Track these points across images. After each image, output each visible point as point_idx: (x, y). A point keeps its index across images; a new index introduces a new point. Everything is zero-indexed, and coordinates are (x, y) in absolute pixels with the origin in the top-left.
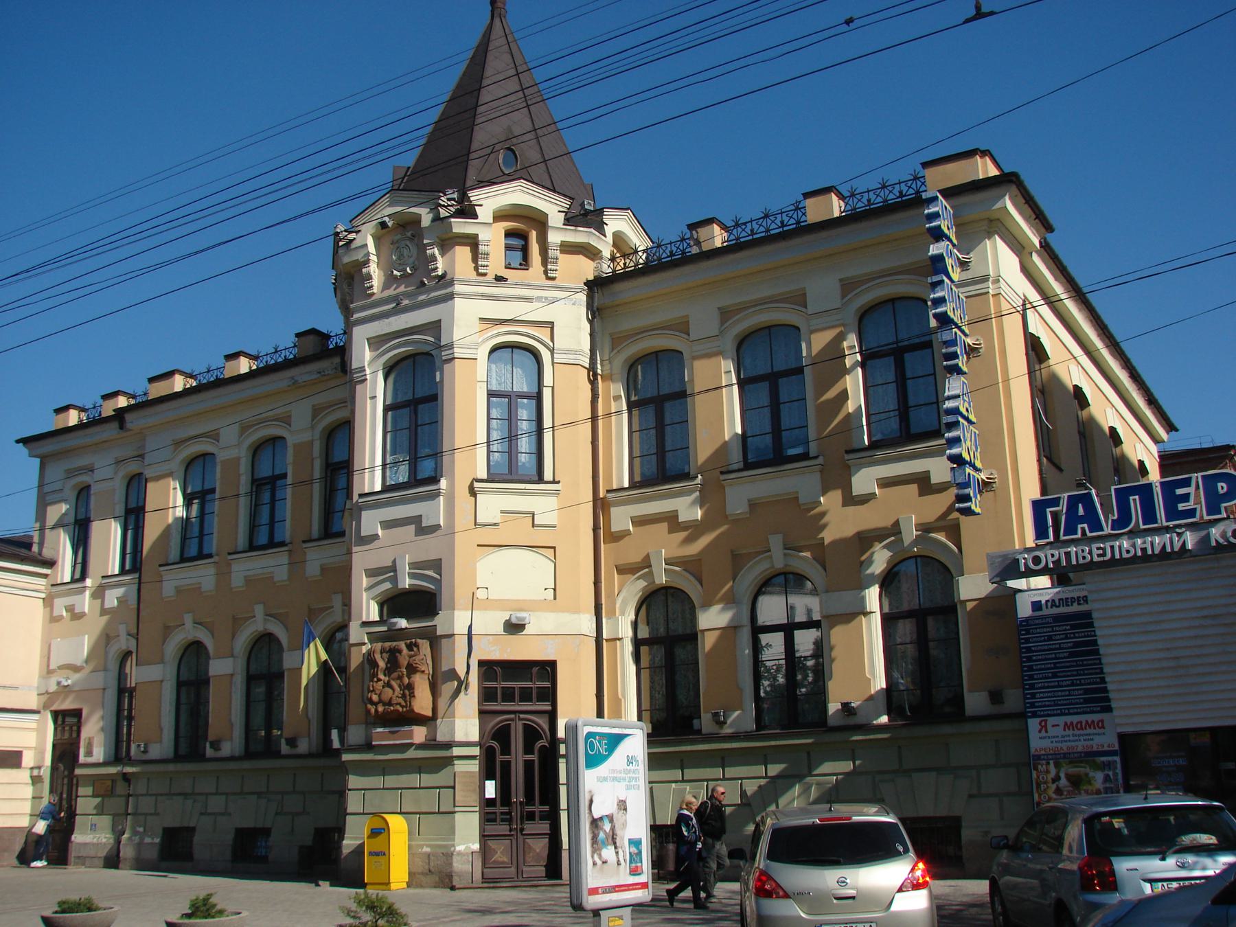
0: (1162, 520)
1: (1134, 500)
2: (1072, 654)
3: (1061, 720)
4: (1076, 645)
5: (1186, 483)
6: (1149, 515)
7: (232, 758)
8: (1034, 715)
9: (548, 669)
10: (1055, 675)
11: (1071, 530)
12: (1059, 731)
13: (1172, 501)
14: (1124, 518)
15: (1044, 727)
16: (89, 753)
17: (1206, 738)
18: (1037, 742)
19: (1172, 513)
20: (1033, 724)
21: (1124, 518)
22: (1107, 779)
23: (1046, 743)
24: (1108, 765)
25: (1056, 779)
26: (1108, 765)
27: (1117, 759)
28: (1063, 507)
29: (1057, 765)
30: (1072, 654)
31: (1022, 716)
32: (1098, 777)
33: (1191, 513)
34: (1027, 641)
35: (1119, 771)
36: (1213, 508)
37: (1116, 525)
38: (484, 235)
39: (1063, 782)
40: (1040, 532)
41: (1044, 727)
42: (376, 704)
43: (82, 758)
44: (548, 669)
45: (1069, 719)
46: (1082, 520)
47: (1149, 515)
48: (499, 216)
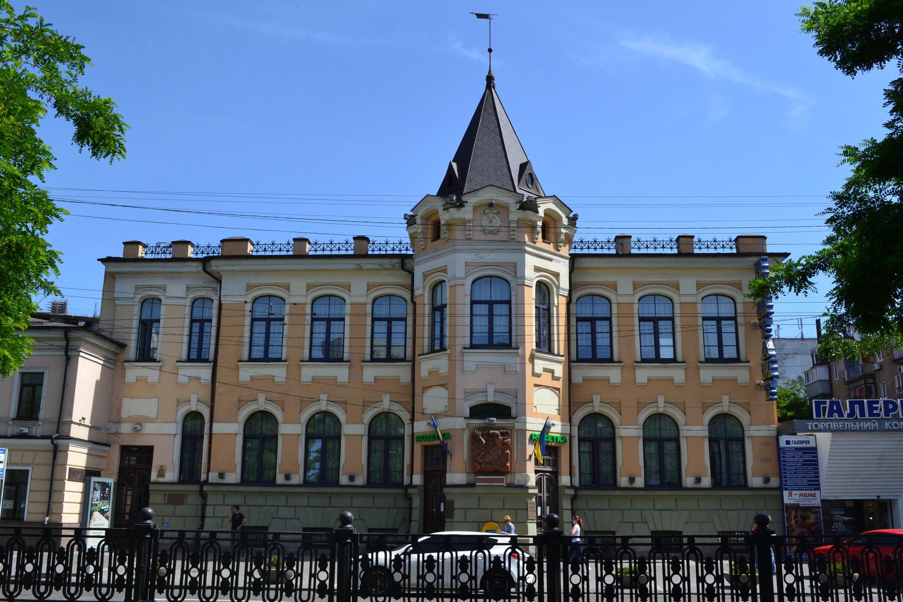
0: (867, 416)
1: (857, 407)
2: (803, 465)
3: (798, 492)
4: (805, 461)
5: (877, 402)
8: (786, 489)
11: (830, 415)
12: (797, 497)
13: (871, 409)
15: (791, 495)
16: (161, 473)
17: (852, 504)
18: (787, 500)
19: (871, 414)
20: (786, 493)
21: (852, 414)
23: (792, 502)
28: (827, 405)
29: (796, 511)
30: (803, 465)
31: (780, 489)
33: (879, 415)
36: (887, 414)
37: (849, 415)
41: (791, 495)
42: (480, 463)
43: (154, 477)
45: (801, 492)
46: (835, 412)
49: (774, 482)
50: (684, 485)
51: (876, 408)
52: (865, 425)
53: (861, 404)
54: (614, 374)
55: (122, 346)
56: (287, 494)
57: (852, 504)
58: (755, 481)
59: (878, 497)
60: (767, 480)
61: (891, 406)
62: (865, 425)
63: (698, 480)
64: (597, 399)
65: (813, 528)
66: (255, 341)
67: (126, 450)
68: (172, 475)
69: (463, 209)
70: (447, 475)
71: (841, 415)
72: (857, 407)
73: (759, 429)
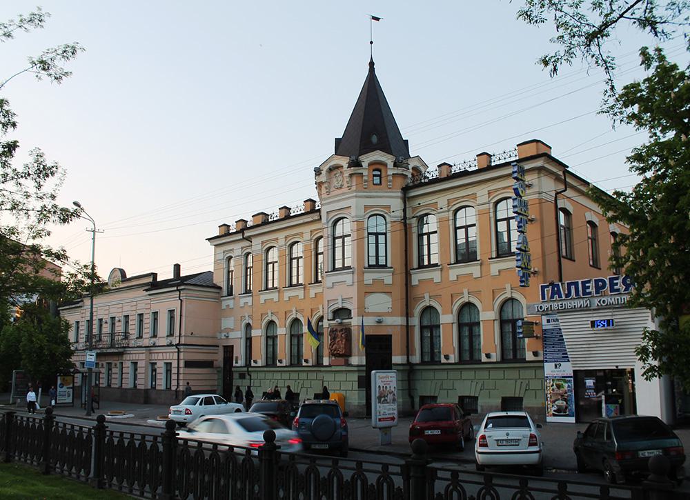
1: (573, 288)
7: (286, 367)
9: (388, 338)
10: (553, 347)
11: (552, 297)
13: (584, 288)
16: (237, 362)
19: (585, 293)
22: (569, 386)
24: (570, 381)
25: (553, 385)
27: (572, 379)
33: (590, 293)
34: (545, 334)
35: (573, 383)
38: (365, 173)
39: (555, 386)
40: (543, 298)
43: (234, 364)
44: (388, 338)
48: (370, 165)
51: (617, 284)
53: (576, 284)
54: (435, 275)
55: (220, 288)
57: (601, 374)
59: (617, 367)
64: (427, 296)
65: (566, 395)
67: (225, 347)
69: (321, 176)
70: (393, 357)
71: (560, 296)
72: (573, 288)
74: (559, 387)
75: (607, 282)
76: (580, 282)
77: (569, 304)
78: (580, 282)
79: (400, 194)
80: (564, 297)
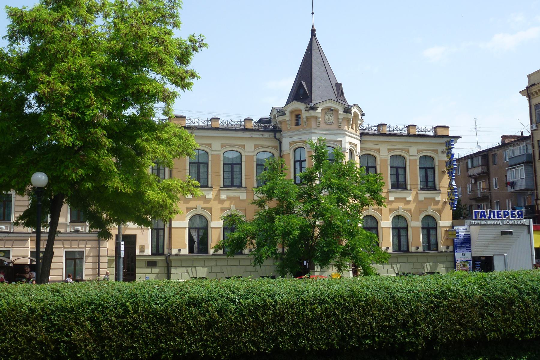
1: (492, 213)
5: (500, 212)
6: (494, 217)
11: (481, 218)
13: (498, 215)
14: (490, 217)
17: (484, 258)
19: (498, 217)
21: (490, 217)
24: (470, 263)
26: (470, 263)
31: (454, 252)
32: (468, 265)
33: (501, 217)
36: (505, 217)
47: (494, 217)
49: (451, 249)
50: (410, 250)
52: (495, 222)
53: (494, 212)
56: (216, 260)
57: (484, 258)
58: (442, 248)
60: (448, 248)
61: (506, 213)
62: (495, 222)
63: (418, 248)
66: (163, 171)
68: (148, 251)
71: (485, 218)
72: (492, 213)
73: (445, 222)
74: (464, 266)
75: (510, 213)
76: (496, 211)
77: (490, 222)
78: (496, 211)
79: (359, 138)
80: (487, 218)
